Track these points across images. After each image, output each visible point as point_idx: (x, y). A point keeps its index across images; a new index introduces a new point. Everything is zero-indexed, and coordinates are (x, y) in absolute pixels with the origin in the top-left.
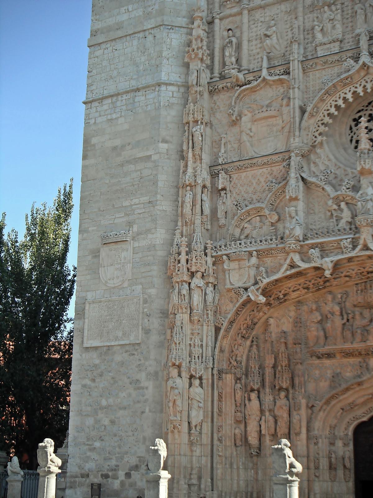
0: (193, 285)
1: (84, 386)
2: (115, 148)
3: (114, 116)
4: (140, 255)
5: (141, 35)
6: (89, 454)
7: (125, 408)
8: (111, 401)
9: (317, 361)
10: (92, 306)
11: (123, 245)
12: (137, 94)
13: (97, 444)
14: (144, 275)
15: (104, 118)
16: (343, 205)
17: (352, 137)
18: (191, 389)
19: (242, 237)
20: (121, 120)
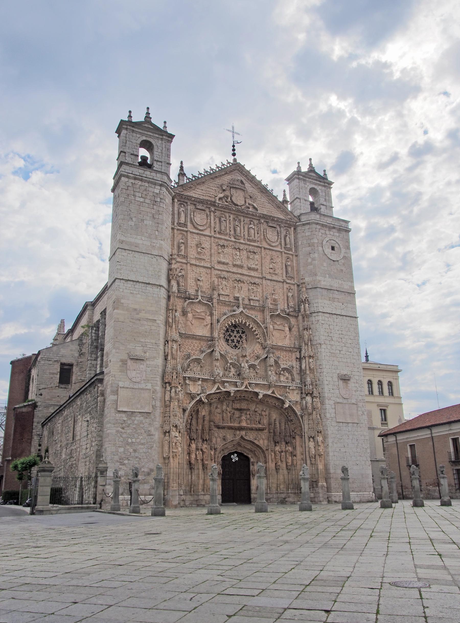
1: (118, 431)
2: (135, 310)
3: (135, 292)
4: (150, 368)
5: (149, 256)
6: (120, 467)
7: (143, 444)
8: (134, 440)
10: (122, 389)
11: (142, 362)
12: (148, 285)
13: (126, 462)
14: (152, 379)
15: (129, 291)
16: (231, 366)
19: (189, 369)
20: (139, 296)
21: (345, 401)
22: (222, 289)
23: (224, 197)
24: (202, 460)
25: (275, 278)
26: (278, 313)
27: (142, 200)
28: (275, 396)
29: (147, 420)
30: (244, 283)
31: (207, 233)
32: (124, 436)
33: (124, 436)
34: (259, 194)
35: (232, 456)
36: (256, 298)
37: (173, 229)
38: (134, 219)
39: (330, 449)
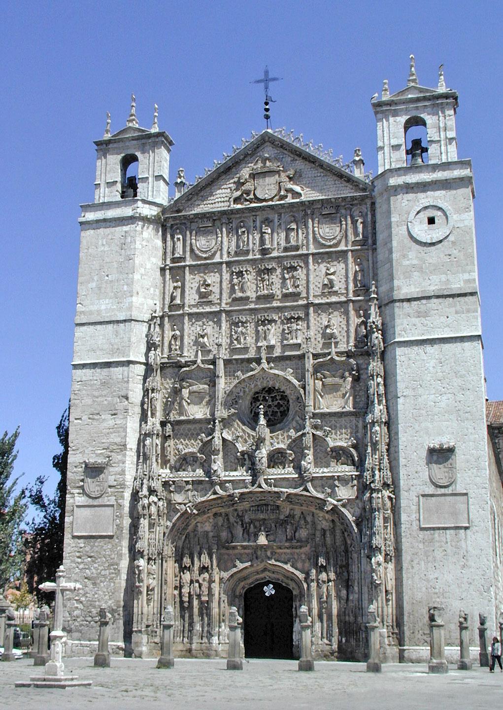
0: (151, 500)
9: (227, 551)
16: (246, 456)
17: (252, 410)
18: (149, 566)
21: (443, 491)
22: (236, 340)
23: (242, 195)
24: (199, 596)
25: (334, 299)
26: (329, 357)
27: (106, 248)
28: (308, 494)
29: (110, 546)
30: (275, 321)
31: (217, 259)
32: (81, 566)
33: (81, 566)
34: (307, 167)
35: (265, 587)
36: (294, 341)
37: (163, 270)
38: (96, 278)
39: (404, 575)
